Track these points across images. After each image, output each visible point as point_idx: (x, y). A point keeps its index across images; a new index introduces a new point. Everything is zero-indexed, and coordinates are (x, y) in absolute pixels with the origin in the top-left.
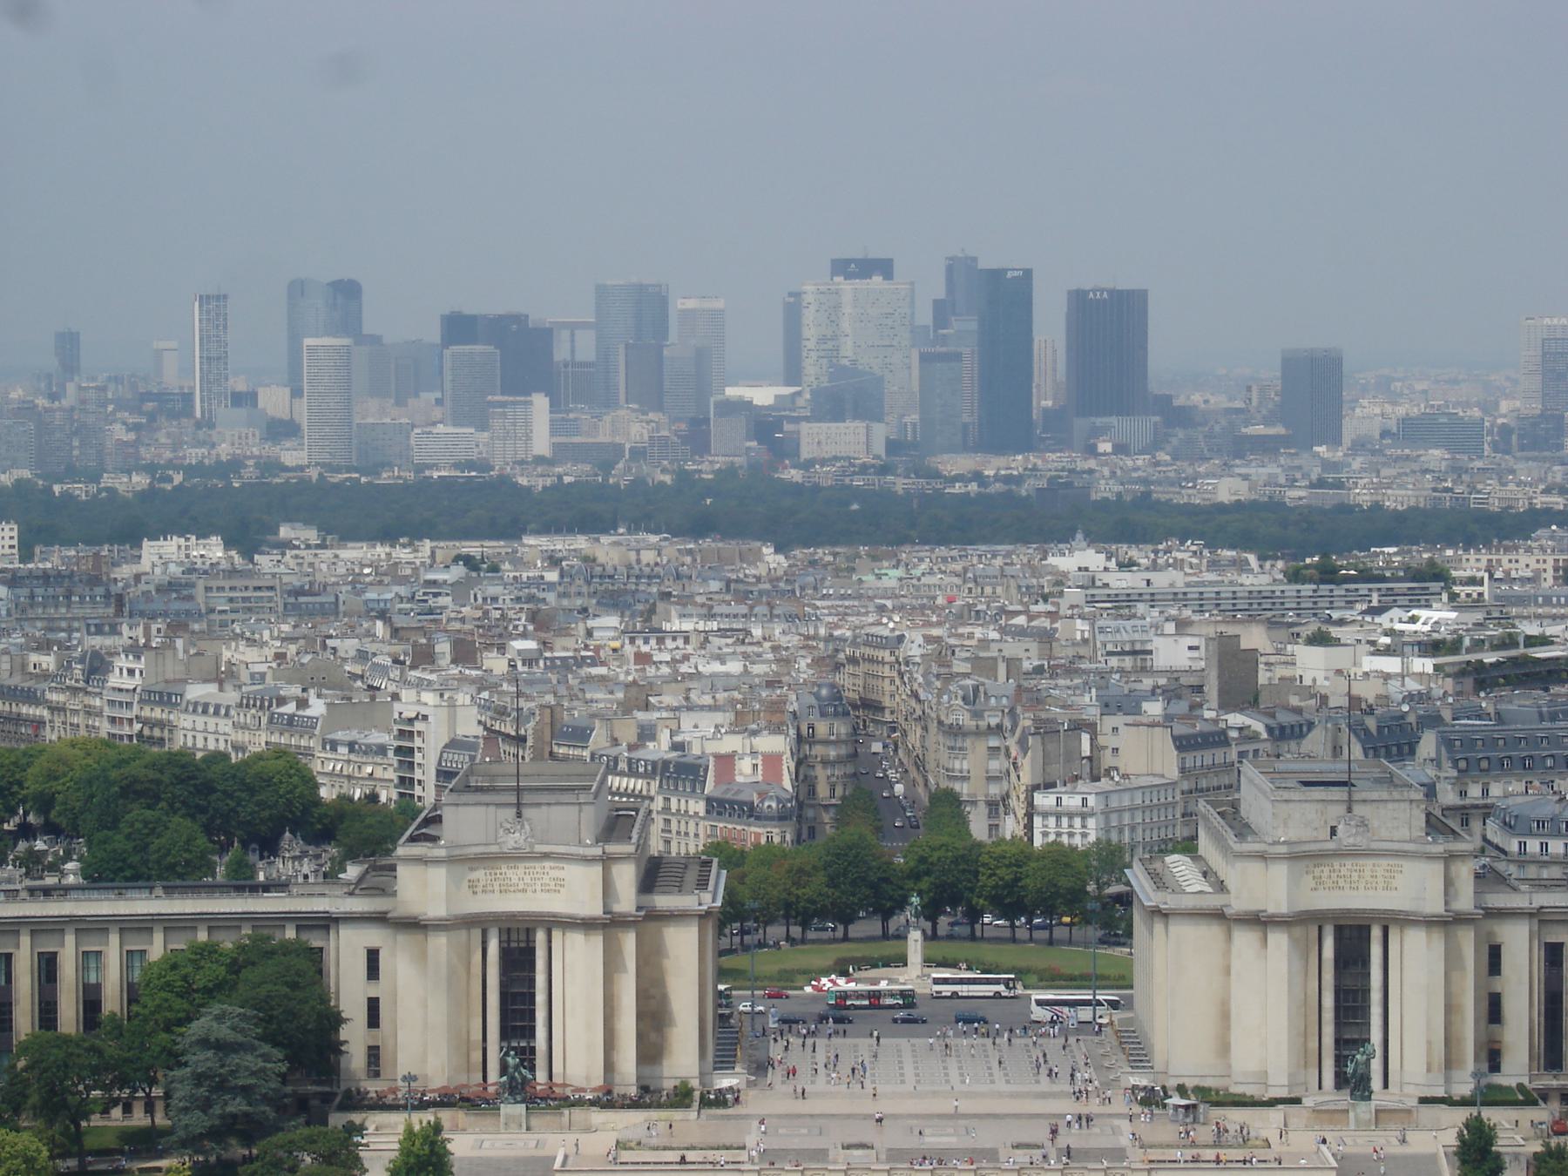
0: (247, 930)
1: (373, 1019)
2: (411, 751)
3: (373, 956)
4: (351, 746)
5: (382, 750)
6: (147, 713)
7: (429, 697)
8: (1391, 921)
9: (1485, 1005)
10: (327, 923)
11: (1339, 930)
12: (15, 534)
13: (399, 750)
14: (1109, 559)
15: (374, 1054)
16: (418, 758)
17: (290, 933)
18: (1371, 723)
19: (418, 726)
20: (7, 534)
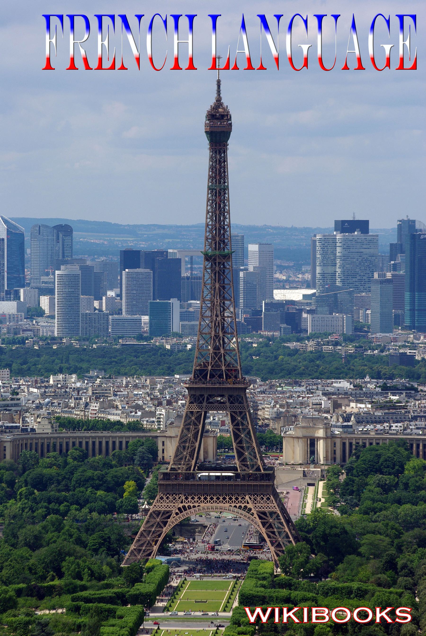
0: (144, 439)
1: (163, 452)
2: (160, 421)
3: (163, 442)
4: (147, 421)
5: (153, 422)
6: (100, 415)
7: (163, 411)
8: (319, 438)
9: (333, 452)
10: (156, 437)
11: (311, 440)
12: (9, 373)
13: (157, 422)
14: (351, 384)
15: (163, 457)
16: (161, 423)
17: (151, 438)
18: (345, 415)
19: (162, 416)
20: (6, 373)
